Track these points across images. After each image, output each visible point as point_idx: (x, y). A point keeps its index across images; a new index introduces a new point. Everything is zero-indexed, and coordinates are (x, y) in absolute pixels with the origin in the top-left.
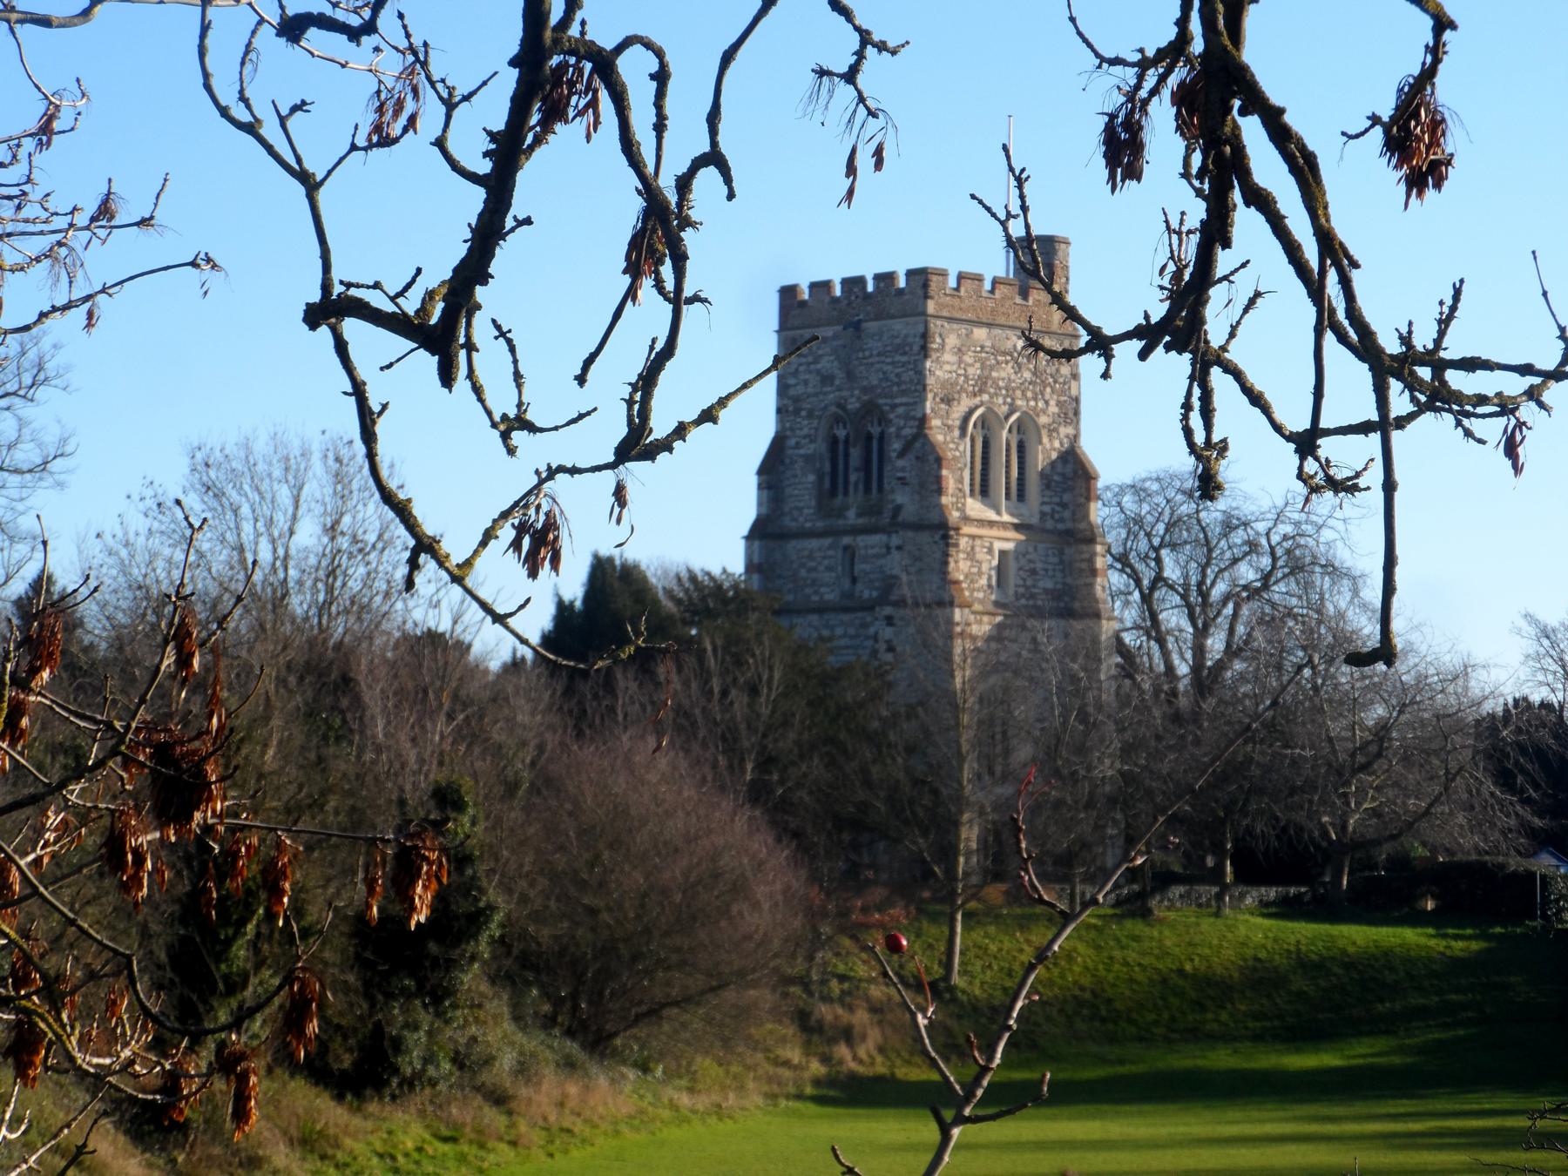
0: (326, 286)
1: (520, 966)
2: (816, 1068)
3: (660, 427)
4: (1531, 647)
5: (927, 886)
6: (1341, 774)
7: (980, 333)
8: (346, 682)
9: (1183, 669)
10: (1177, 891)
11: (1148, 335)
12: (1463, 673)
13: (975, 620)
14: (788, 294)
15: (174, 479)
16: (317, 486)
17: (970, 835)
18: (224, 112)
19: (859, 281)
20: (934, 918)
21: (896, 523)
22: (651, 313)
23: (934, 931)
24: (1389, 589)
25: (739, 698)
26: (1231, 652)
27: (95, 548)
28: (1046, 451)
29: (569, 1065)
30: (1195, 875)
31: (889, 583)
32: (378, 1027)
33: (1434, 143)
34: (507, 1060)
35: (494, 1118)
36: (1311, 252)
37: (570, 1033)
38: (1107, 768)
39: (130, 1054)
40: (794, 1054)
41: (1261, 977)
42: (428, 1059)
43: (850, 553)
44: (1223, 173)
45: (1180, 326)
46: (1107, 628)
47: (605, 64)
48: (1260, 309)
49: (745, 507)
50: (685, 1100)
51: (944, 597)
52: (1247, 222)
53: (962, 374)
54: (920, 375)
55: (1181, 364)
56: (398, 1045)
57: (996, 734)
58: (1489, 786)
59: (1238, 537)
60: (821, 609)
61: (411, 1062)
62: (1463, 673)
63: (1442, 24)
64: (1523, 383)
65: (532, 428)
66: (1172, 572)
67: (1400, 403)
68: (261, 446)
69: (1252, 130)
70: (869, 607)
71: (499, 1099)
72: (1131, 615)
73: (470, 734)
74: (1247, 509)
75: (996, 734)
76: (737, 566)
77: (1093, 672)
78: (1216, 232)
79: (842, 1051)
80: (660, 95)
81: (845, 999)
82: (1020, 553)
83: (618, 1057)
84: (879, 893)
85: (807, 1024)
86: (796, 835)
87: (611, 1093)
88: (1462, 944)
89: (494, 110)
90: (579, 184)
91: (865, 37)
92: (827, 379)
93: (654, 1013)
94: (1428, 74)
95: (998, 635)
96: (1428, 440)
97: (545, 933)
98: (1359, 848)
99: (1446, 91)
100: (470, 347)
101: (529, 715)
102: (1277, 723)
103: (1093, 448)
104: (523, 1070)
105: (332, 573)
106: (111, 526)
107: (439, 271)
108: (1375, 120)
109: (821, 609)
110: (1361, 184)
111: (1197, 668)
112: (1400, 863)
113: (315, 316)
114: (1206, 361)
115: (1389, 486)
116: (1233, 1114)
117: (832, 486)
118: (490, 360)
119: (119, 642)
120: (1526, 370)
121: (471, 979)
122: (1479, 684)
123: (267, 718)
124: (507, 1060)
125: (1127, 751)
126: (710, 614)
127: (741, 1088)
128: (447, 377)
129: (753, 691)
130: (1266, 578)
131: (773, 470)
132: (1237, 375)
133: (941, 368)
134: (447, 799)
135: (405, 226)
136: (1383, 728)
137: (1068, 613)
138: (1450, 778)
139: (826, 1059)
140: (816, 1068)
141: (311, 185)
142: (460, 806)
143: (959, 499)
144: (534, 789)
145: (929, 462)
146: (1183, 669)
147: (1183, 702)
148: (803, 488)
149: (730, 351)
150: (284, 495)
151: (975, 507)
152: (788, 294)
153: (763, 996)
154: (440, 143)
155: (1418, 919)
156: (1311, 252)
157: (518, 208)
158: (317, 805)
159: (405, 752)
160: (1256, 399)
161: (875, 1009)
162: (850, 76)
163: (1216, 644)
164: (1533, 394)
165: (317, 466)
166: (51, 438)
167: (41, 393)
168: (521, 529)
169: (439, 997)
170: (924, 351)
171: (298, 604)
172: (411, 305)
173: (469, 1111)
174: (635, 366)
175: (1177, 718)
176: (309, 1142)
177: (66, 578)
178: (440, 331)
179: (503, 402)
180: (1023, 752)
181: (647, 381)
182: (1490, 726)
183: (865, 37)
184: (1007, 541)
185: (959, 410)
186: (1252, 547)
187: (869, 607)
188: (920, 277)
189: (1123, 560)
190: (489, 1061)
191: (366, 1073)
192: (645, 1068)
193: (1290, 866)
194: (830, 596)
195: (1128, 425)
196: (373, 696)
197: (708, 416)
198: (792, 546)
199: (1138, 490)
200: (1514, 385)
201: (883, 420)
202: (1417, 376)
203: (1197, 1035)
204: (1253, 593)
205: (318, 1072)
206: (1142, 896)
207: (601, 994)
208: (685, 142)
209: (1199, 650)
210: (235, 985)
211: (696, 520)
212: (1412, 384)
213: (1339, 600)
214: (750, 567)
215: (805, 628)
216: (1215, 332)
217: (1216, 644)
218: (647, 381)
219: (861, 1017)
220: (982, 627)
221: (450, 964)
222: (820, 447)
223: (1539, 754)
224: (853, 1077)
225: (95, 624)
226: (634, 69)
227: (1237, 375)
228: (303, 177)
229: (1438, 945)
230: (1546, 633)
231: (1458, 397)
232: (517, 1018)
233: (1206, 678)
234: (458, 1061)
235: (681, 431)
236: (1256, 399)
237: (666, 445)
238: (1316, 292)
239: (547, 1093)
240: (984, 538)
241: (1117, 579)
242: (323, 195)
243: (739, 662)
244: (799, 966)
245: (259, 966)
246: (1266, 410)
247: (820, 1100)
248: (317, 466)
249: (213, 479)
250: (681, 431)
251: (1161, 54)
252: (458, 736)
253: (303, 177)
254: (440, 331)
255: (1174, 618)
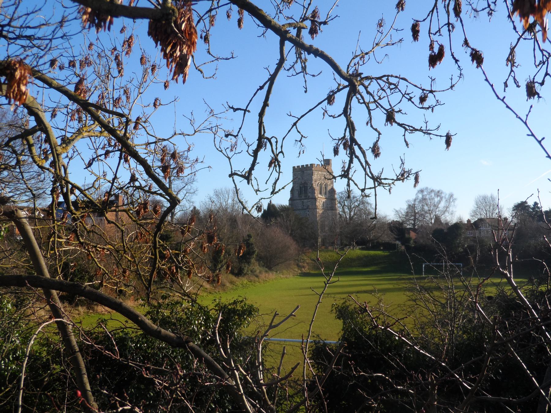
0: (232, 172)
1: (260, 259)
2: (300, 271)
3: (276, 190)
4: (395, 213)
5: (314, 247)
6: (370, 231)
7: (320, 172)
8: (235, 221)
9: (348, 217)
10: (348, 247)
11: (342, 176)
12: (385, 217)
13: (320, 211)
14: (294, 167)
15: (212, 194)
16: (231, 194)
17: (320, 240)
18: (217, 149)
19: (303, 166)
20: (315, 251)
21: (309, 198)
22: (275, 175)
23: (315, 253)
24: (376, 205)
25: (288, 222)
26: (354, 214)
27: (201, 203)
28: (329, 188)
29: (266, 272)
30: (350, 245)
31: (308, 206)
32: (241, 267)
33: (378, 151)
34: (258, 271)
35: (256, 279)
36: (364, 164)
37: (266, 267)
38: (338, 230)
39: (206, 272)
40: (297, 270)
41: (359, 258)
42: (248, 271)
43: (303, 202)
44: (352, 154)
45: (346, 174)
46: (338, 212)
47: (269, 140)
48: (358, 173)
49: (288, 196)
50: (282, 276)
51: (315, 208)
52: (355, 160)
53: (317, 177)
54: (312, 178)
55: (346, 180)
56: (243, 269)
57: (323, 226)
58: (390, 232)
59: (355, 199)
60: (299, 210)
61: (245, 271)
62: (385, 217)
63: (380, 134)
64: (391, 181)
65: (260, 191)
66: (346, 204)
67: (376, 185)
68: (223, 189)
69: (356, 148)
70: (305, 209)
71: (257, 276)
72: (341, 210)
73: (252, 227)
74: (356, 195)
75: (323, 226)
76: (288, 204)
77: (336, 217)
78: (351, 162)
79: (303, 269)
80: (276, 145)
81: (303, 262)
82: (326, 202)
83: (273, 270)
84: (307, 248)
85: (298, 266)
86: (296, 240)
87: (272, 275)
88: (386, 253)
89: (254, 147)
90: (265, 155)
91: (302, 136)
92: (299, 179)
93: (278, 264)
94: (377, 141)
95: (323, 213)
96: (379, 189)
97: (263, 254)
98: (372, 241)
99: (380, 144)
100: (251, 180)
101: (261, 222)
102: (361, 225)
103: (335, 187)
104: (260, 272)
105: (233, 206)
106: (203, 200)
107: (247, 169)
108: (370, 148)
109: (299, 210)
110: (370, 155)
111: (350, 217)
112: (378, 242)
113: (231, 176)
114: (349, 179)
115: (376, 195)
116: (356, 277)
117: (300, 194)
118: (254, 182)
119: (205, 216)
120: (392, 180)
121: (253, 260)
122: (388, 218)
123: (225, 226)
124: (258, 271)
125: (341, 228)
126: (284, 211)
127: (289, 274)
128: (248, 183)
129: (290, 221)
130: (359, 205)
131: (292, 191)
132: (353, 181)
133: (315, 177)
134: (249, 236)
135: (242, 163)
136: (375, 225)
137: (332, 210)
138: (384, 231)
139: (301, 270)
140: (300, 271)
141: (229, 159)
142: (251, 237)
143: (317, 195)
144: (261, 235)
145: (313, 190)
146: (348, 217)
147: (348, 221)
148: (296, 193)
149: (287, 178)
150: (227, 196)
151: (320, 196)
152: (294, 167)
153: (292, 262)
154: (247, 151)
155: (380, 250)
156: (364, 164)
157: (257, 161)
158: (232, 237)
159: (244, 230)
160: (356, 185)
161: (307, 263)
162: (300, 141)
163: (352, 213)
164: (393, 183)
165: (231, 192)
166: (195, 189)
167: (194, 183)
168: (257, 207)
169: (249, 263)
170: (312, 175)
171: (229, 210)
172: (243, 173)
173: (253, 278)
174: (274, 181)
175: (347, 224)
176: (232, 283)
177: (198, 208)
178: (248, 177)
179: (256, 188)
180: (327, 229)
181: (275, 183)
182: (389, 224)
183: (302, 136)
184: (324, 200)
185: (317, 183)
186: (357, 200)
187: (305, 209)
188: (312, 165)
189: (340, 202)
190: (256, 271)
191: (239, 273)
192: (276, 272)
193: (363, 243)
194: (300, 208)
195: (340, 186)
196: (239, 222)
197: (283, 188)
198: (295, 201)
199: (341, 193)
200: (390, 182)
201: (307, 184)
202: (377, 180)
203: (352, 267)
204: (357, 206)
205: (232, 273)
206: (343, 248)
207: (270, 262)
208: (279, 150)
209: (350, 214)
210: (221, 262)
211: (283, 199)
212: (378, 181)
213: (369, 207)
214: (289, 204)
215: (297, 212)
216: (350, 176)
217: (352, 213)
218: (275, 183)
219: (305, 265)
220: (321, 212)
221: (250, 258)
222: (298, 188)
223: (396, 228)
224: (305, 273)
225: (202, 214)
226: (273, 141)
227: (353, 181)
228: (228, 157)
229: (383, 253)
230: (397, 211)
231: (383, 184)
232: (259, 265)
233: (351, 218)
234: (251, 271)
235: (279, 190)
236: (356, 185)
237: (277, 192)
238: (365, 170)
239: (263, 275)
240: (321, 200)
241: (339, 205)
242: (231, 160)
243: (288, 217)
244: (297, 258)
245: (225, 259)
246: (357, 186)
247: (300, 276)
248: (231, 192)
249: (217, 194)
250: (279, 190)
251: (342, 138)
252: (251, 228)
253: (228, 157)
254: (248, 177)
255: (347, 210)
